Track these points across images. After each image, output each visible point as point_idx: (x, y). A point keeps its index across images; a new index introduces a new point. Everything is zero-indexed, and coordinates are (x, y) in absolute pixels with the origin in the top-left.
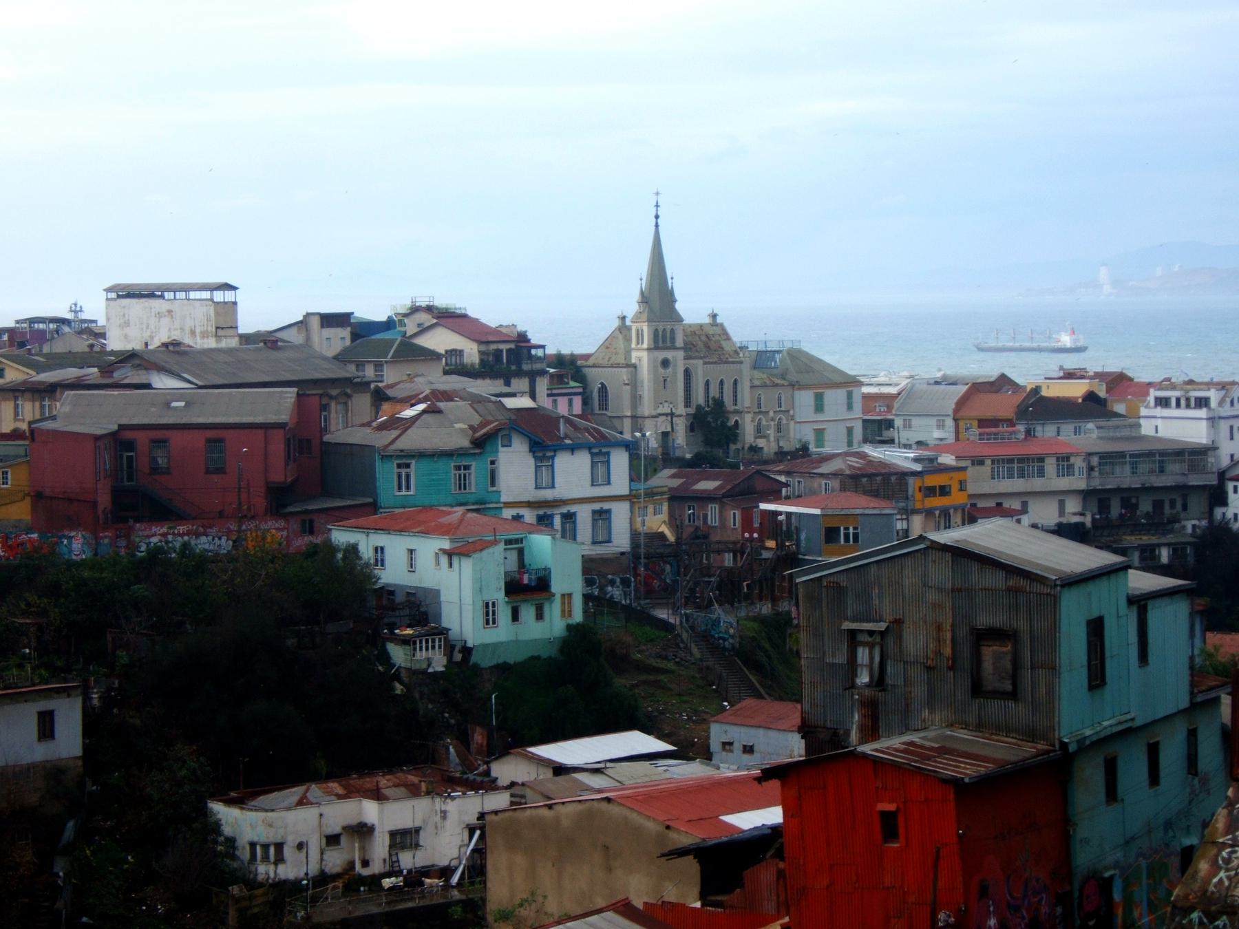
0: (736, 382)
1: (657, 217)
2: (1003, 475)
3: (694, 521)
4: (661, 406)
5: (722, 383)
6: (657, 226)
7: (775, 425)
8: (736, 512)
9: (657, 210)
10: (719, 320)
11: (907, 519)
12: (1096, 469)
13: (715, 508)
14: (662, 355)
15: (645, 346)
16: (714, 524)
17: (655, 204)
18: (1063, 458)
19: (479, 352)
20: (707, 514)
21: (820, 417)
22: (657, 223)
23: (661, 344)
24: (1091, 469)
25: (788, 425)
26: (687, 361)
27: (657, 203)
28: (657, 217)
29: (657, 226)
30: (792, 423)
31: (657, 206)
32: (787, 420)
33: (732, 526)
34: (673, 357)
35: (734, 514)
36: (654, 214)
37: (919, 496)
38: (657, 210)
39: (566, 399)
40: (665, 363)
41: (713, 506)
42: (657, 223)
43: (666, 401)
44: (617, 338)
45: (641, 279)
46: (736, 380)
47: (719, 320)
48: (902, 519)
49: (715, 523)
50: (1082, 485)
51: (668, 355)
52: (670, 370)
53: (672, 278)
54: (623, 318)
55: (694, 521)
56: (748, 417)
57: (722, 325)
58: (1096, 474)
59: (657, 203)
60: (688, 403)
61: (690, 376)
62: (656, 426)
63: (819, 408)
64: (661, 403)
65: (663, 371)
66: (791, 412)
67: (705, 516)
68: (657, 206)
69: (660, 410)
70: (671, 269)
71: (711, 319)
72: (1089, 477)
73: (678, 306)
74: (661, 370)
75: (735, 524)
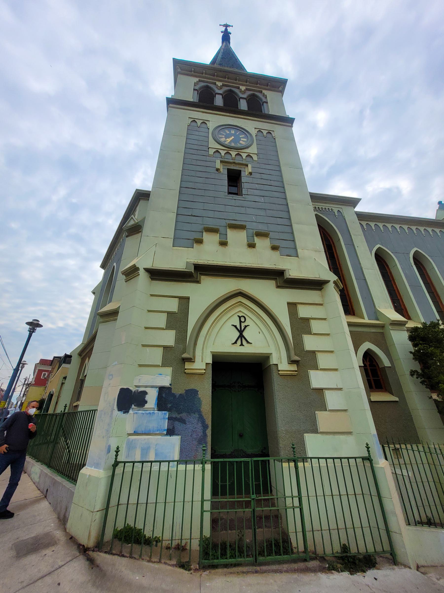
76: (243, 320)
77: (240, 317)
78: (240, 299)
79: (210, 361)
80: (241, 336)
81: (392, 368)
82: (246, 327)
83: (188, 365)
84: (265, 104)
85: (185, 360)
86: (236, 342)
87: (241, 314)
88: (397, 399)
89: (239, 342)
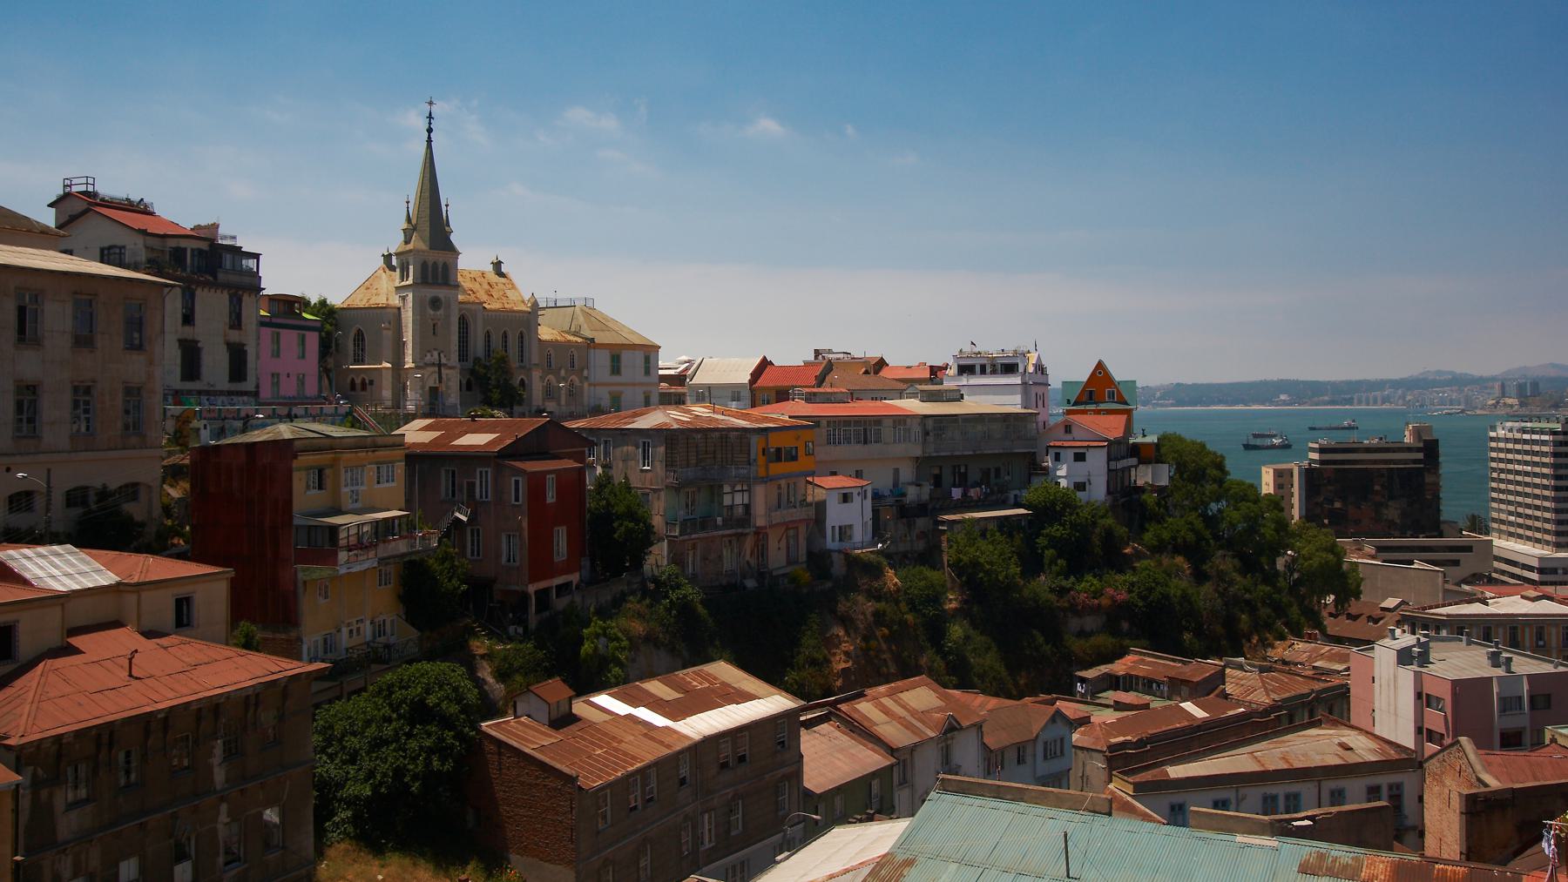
0: (521, 336)
1: (430, 130)
2: (840, 439)
3: (453, 495)
4: (429, 355)
5: (505, 335)
6: (429, 141)
8: (520, 479)
9: (430, 123)
11: (749, 491)
12: (931, 434)
13: (486, 472)
14: (431, 292)
15: (410, 281)
16: (484, 499)
18: (900, 421)
19: (147, 248)
20: (473, 484)
21: (616, 379)
22: (429, 137)
23: (430, 280)
24: (927, 433)
25: (582, 387)
27: (430, 113)
28: (430, 130)
29: (429, 141)
30: (586, 385)
31: (430, 117)
32: (581, 382)
33: (513, 502)
34: (445, 297)
35: (517, 482)
37: (762, 460)
38: (430, 123)
39: (295, 332)
40: (435, 303)
41: (484, 470)
42: (429, 137)
43: (435, 349)
44: (380, 278)
45: (408, 202)
46: (521, 336)
48: (743, 491)
49: (486, 497)
50: (918, 452)
51: (441, 293)
53: (447, 206)
54: (383, 255)
55: (453, 495)
56: (536, 374)
58: (931, 438)
59: (430, 113)
60: (463, 356)
61: (467, 324)
63: (616, 369)
64: (429, 351)
65: (432, 312)
66: (585, 373)
67: (471, 486)
68: (430, 117)
69: (428, 358)
70: (444, 195)
72: (925, 442)
73: (453, 238)
75: (517, 500)
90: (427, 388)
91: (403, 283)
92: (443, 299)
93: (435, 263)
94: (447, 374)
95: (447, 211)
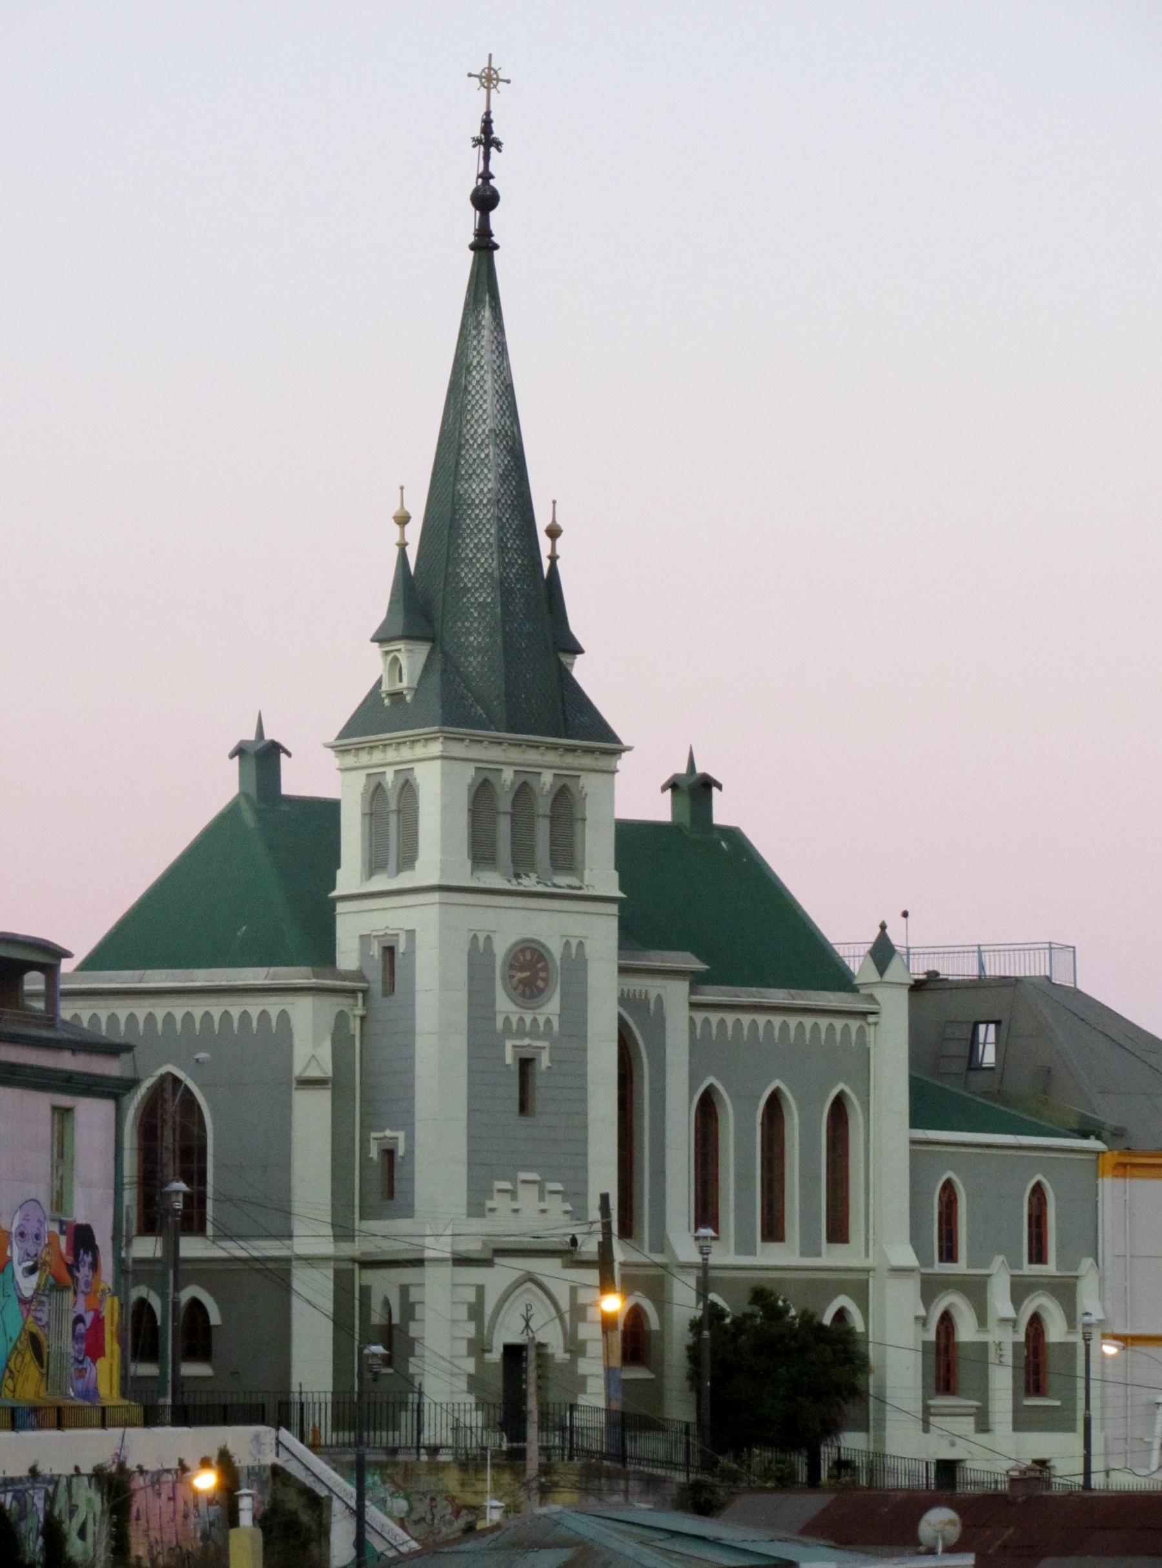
6: (484, 245)
7: (1016, 1345)
10: (723, 812)
17: (477, 132)
26: (638, 984)
27: (487, 125)
29: (484, 245)
31: (487, 141)
36: (471, 183)
39: (41, 1103)
47: (723, 812)
52: (553, 1006)
53: (554, 533)
57: (733, 835)
59: (487, 125)
62: (476, 1312)
68: (487, 141)
71: (686, 801)
73: (582, 671)
74: (504, 1005)
76: (529, 1308)
77: (527, 1306)
78: (529, 1285)
79: (501, 1349)
80: (527, 1326)
81: (660, 1334)
82: (532, 1315)
83: (487, 1356)
84: (580, 823)
85: (484, 1351)
86: (522, 1333)
87: (527, 1302)
88: (652, 1376)
89: (525, 1332)
90: (496, 1356)
91: (380, 883)
92: (555, 948)
93: (523, 792)
94: (574, 1291)
95: (553, 558)
